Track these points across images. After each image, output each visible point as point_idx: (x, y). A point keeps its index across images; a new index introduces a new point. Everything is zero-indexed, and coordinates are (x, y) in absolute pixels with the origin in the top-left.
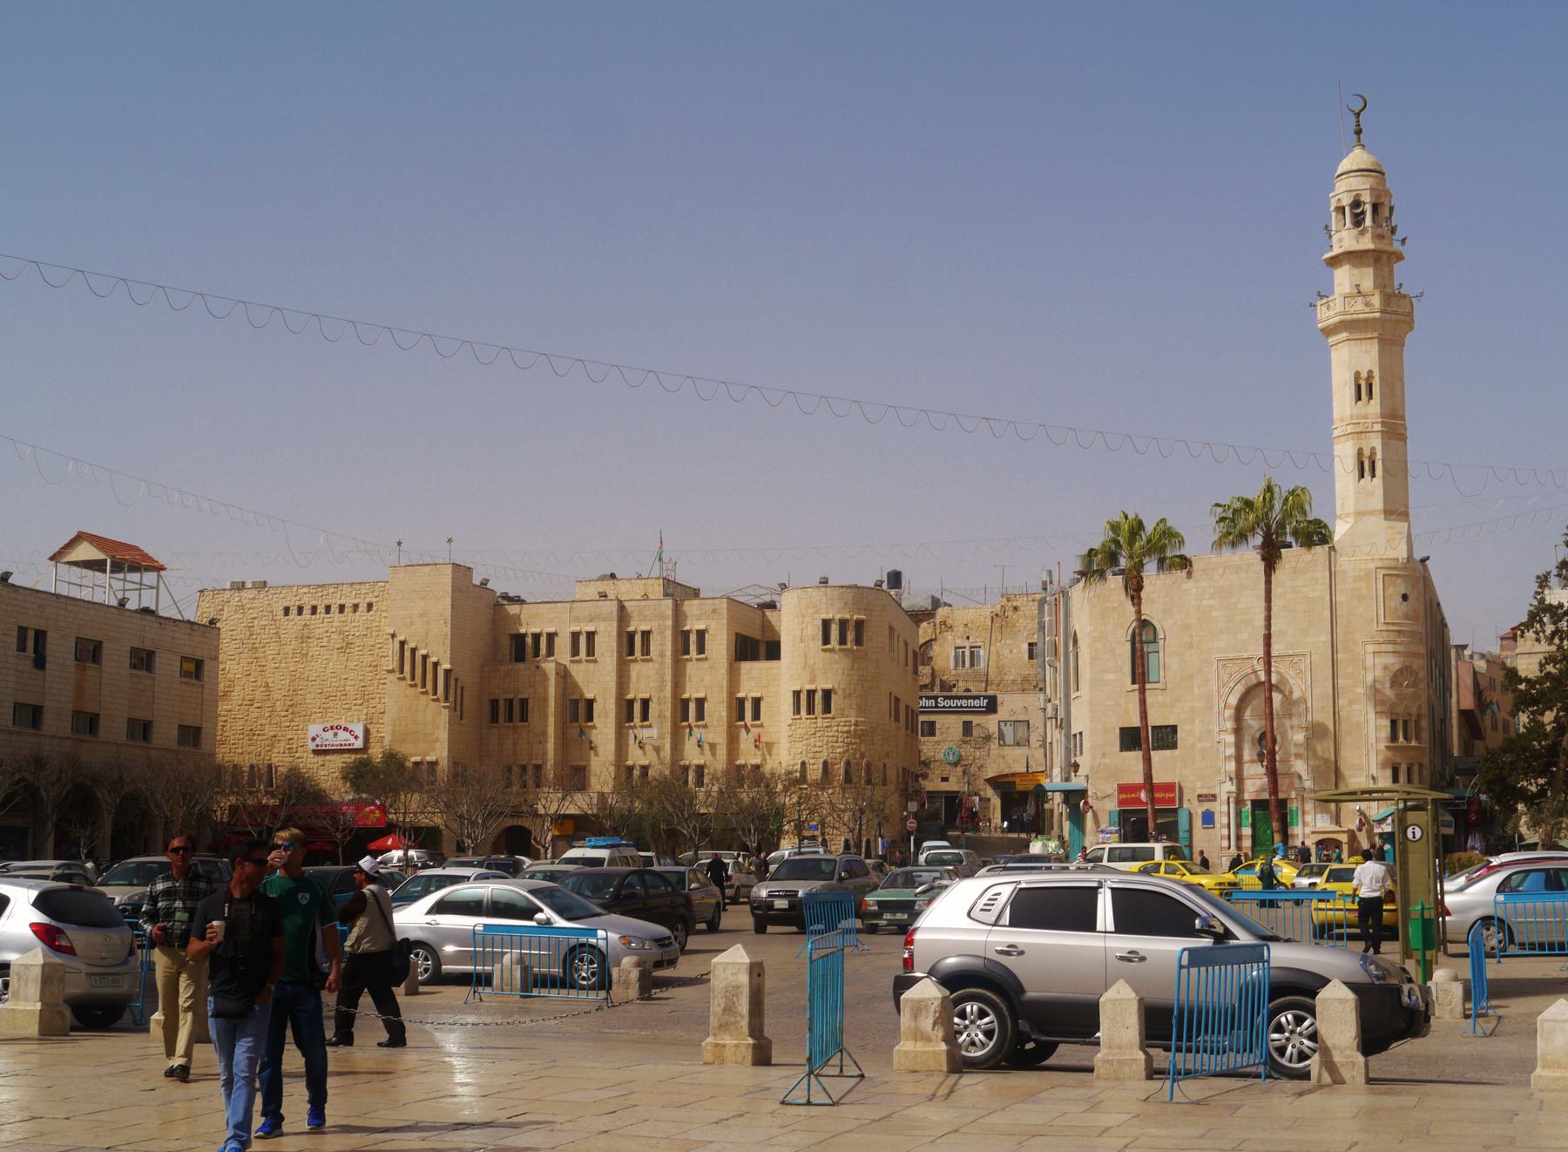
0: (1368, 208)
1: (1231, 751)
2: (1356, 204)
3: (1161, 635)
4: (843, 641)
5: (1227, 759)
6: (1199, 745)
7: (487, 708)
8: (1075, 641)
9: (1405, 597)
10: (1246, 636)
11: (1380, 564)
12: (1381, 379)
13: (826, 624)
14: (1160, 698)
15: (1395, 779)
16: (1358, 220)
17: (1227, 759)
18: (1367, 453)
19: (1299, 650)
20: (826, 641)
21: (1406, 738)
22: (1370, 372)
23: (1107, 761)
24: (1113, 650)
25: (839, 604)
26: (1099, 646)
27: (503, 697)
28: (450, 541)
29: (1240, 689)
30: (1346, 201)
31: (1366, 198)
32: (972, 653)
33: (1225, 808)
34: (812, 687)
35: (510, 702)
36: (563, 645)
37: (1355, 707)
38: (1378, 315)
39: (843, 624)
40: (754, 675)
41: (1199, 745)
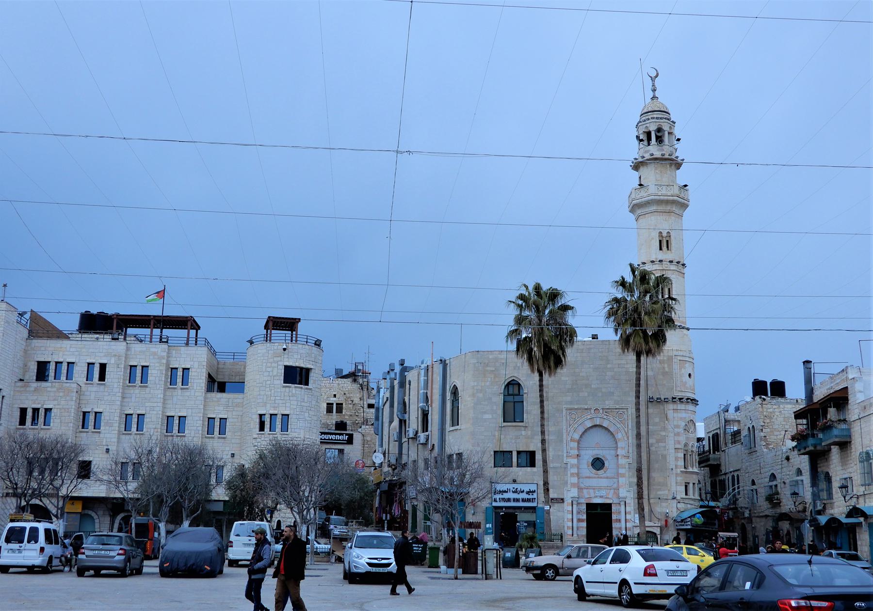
0: (666, 133)
2: (659, 130)
5: (572, 475)
7: (17, 414)
8: (455, 392)
9: (690, 375)
10: (586, 394)
15: (686, 494)
17: (572, 475)
26: (481, 395)
27: (30, 405)
28: (5, 286)
29: (581, 430)
33: (570, 508)
34: (275, 412)
35: (36, 411)
36: (80, 372)
40: (221, 405)
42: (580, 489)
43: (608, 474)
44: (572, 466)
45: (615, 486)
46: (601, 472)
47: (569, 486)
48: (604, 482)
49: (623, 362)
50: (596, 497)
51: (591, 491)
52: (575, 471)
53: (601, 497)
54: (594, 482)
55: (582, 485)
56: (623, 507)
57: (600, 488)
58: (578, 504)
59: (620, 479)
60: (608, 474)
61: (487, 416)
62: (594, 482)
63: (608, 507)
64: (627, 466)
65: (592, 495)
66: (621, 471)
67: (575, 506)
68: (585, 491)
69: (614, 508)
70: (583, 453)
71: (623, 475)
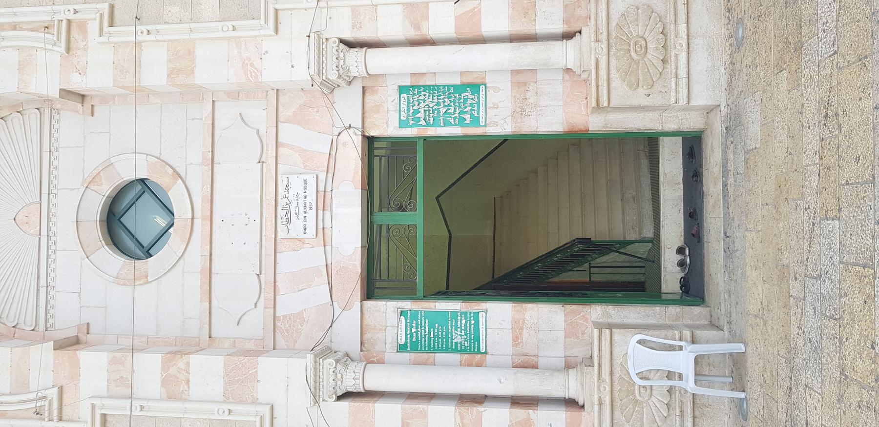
42: (274, 340)
43: (190, 158)
44: (124, 386)
45: (259, 114)
46: (177, 198)
47: (244, 412)
48: (239, 188)
50: (323, 234)
51: (288, 262)
52: (149, 368)
53: (323, 202)
54: (238, 248)
55: (256, 323)
56: (377, 60)
57: (277, 210)
58: (369, 356)
59: (204, 76)
60: (190, 158)
62: (238, 248)
63: (387, 165)
64: (124, 33)
65: (314, 257)
66: (155, 73)
67: (376, 379)
68: (288, 304)
69: (389, 126)
70: (66, 320)
71: (182, 59)
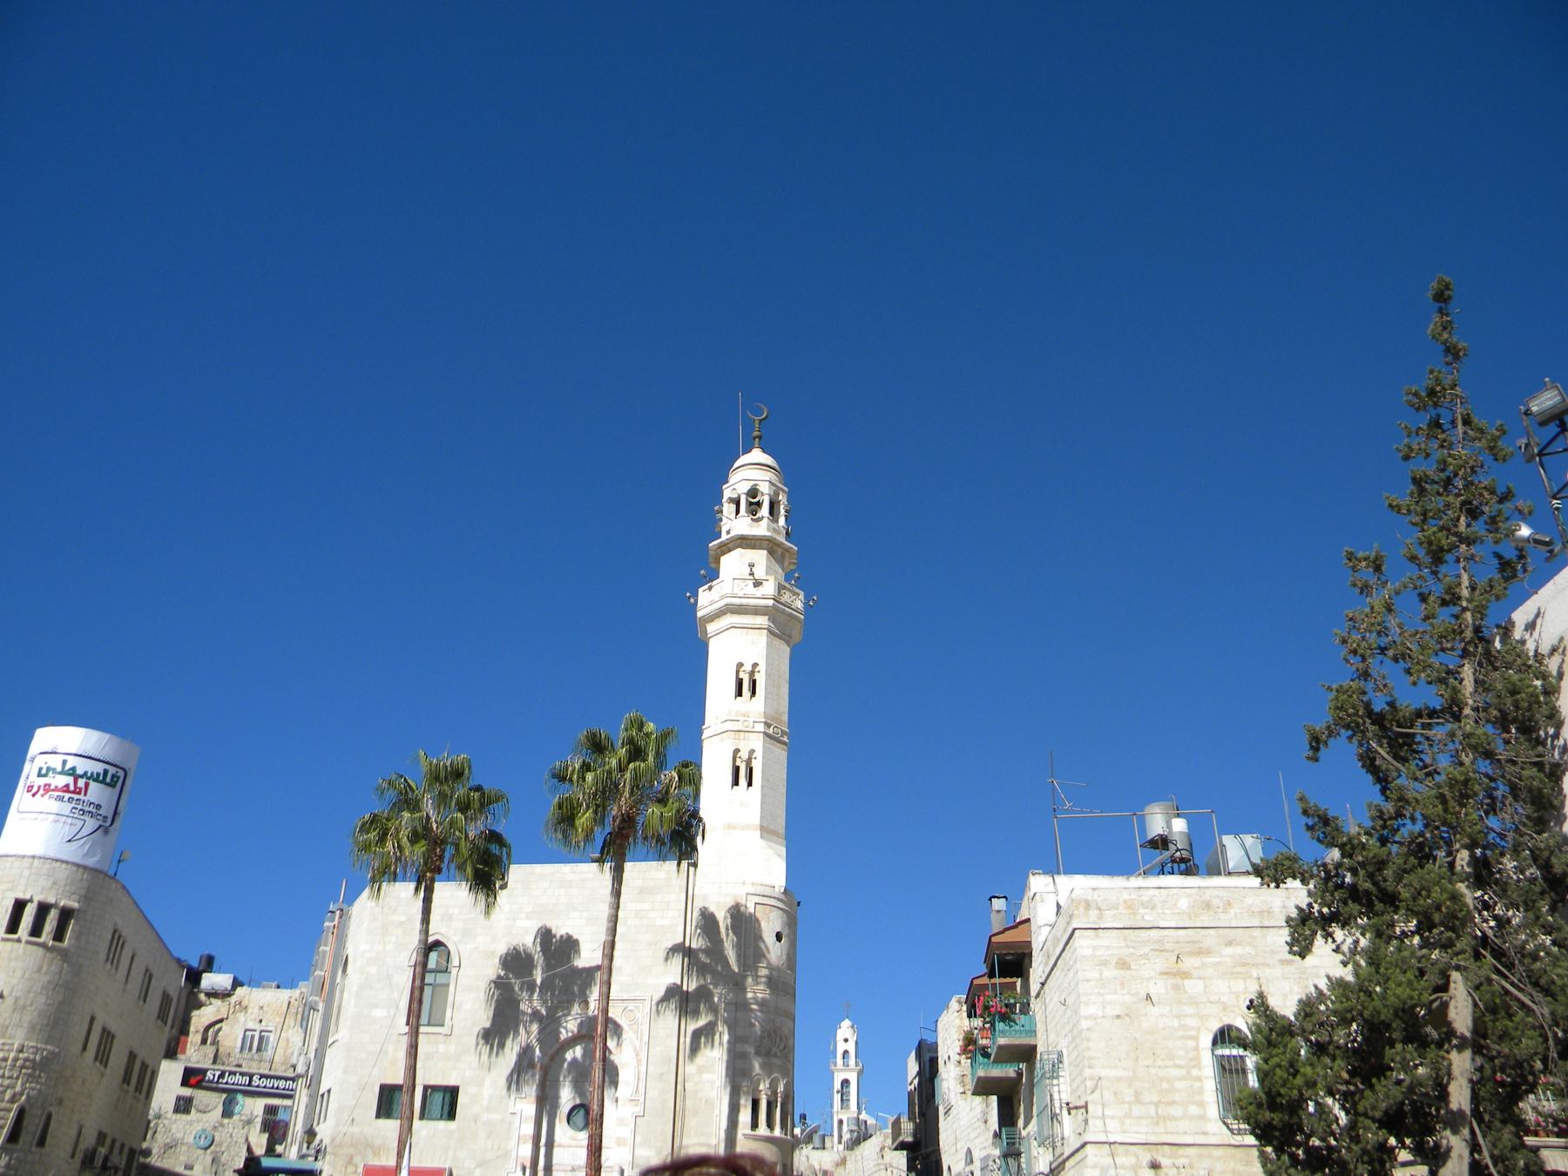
1: (529, 1129)
2: (753, 492)
3: (455, 962)
4: (36, 930)
6: (485, 1117)
11: (752, 890)
12: (768, 675)
13: (20, 906)
14: (442, 1048)
16: (754, 508)
18: (744, 755)
19: (637, 994)
20: (13, 927)
21: (770, 1125)
22: (755, 665)
23: (355, 1129)
24: (389, 978)
25: (44, 882)
26: (373, 970)
30: (743, 488)
31: (765, 488)
32: (261, 1038)
37: (706, 1076)
38: (771, 602)
39: (43, 909)
41: (485, 1117)
49: (646, 906)
61: (379, 1013)
